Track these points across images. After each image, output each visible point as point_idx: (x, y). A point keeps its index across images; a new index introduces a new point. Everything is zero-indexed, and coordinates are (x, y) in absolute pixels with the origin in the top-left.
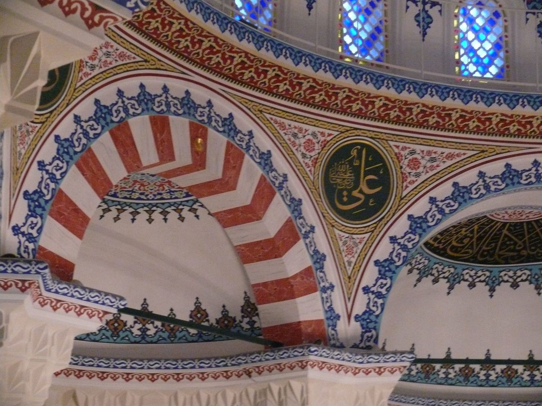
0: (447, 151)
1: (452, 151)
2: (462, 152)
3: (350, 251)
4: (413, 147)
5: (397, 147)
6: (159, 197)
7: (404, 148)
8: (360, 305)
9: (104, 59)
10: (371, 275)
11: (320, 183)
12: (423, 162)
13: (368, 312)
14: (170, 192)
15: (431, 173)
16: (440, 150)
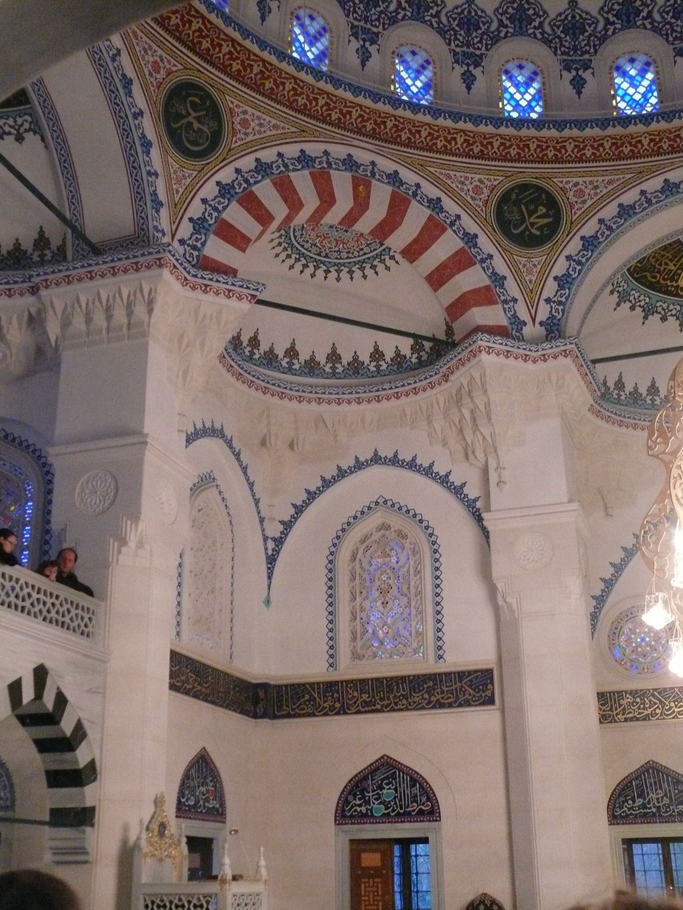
0: (607, 178)
1: (612, 177)
2: (621, 176)
3: (530, 272)
4: (575, 180)
5: (562, 182)
6: (362, 253)
7: (567, 183)
8: (543, 312)
9: (257, 128)
10: (550, 288)
11: (492, 219)
12: (587, 191)
13: (552, 317)
14: (368, 245)
15: (596, 199)
16: (600, 179)
